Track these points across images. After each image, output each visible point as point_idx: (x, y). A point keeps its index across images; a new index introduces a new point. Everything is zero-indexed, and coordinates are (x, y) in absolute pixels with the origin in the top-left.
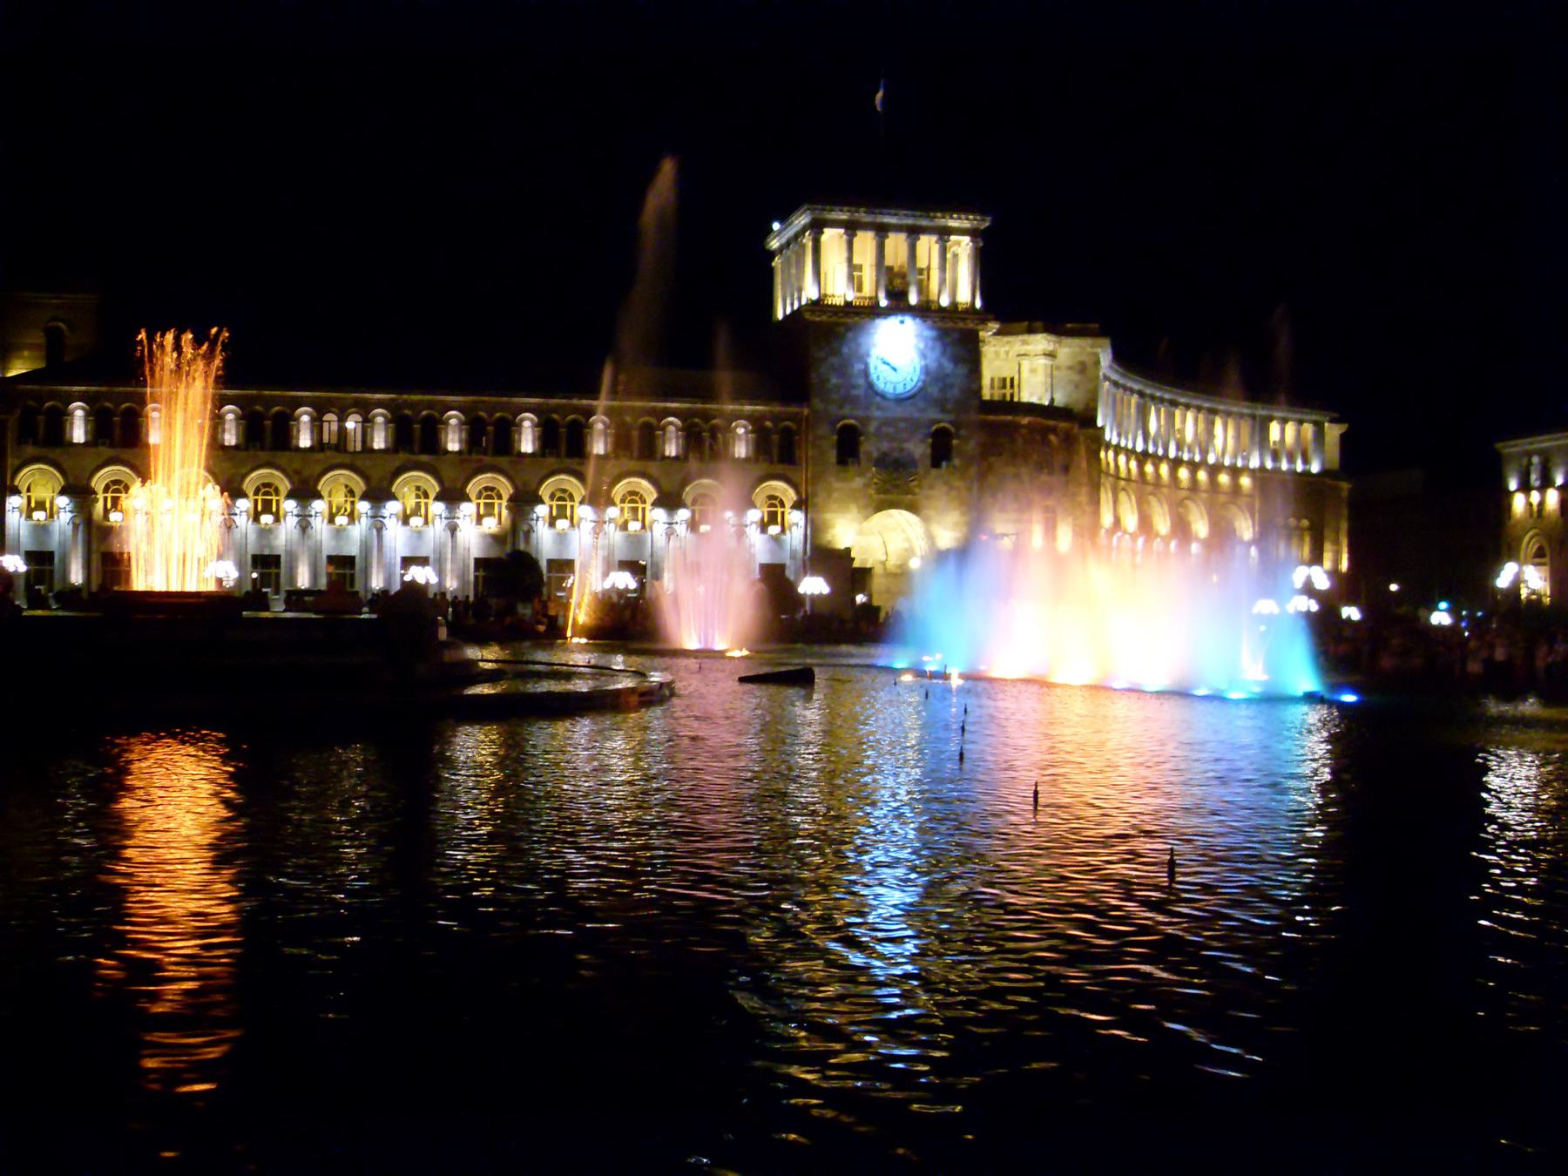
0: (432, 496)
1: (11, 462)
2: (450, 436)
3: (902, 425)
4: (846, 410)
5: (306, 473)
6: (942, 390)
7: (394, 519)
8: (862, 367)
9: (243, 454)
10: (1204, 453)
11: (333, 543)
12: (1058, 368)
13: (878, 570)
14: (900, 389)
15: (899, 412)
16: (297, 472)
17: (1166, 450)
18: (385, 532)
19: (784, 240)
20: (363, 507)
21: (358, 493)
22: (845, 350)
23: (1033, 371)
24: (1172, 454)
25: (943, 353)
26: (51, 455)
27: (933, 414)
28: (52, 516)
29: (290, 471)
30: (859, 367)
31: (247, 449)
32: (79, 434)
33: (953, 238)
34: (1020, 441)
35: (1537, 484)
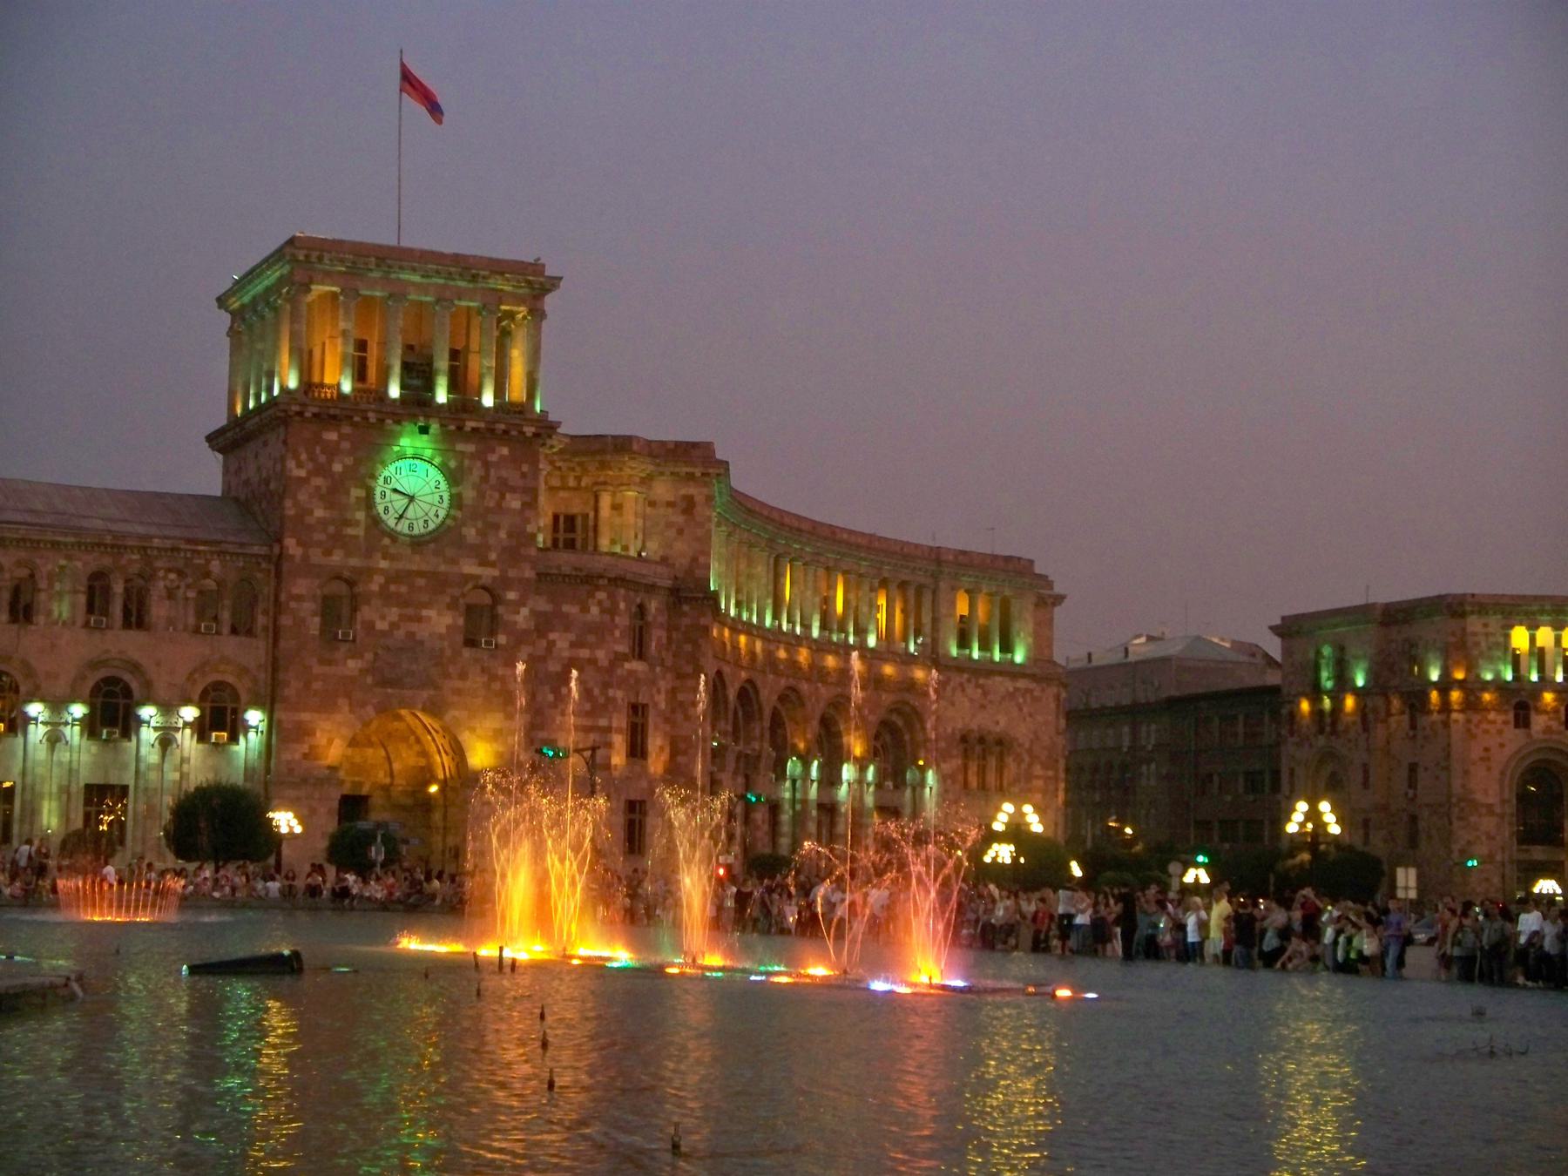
3: (421, 582)
4: (337, 557)
6: (482, 533)
8: (361, 493)
10: (861, 632)
12: (652, 504)
13: (377, 800)
14: (419, 529)
15: (416, 563)
17: (807, 627)
19: (246, 299)
22: (337, 467)
23: (617, 507)
24: (815, 633)
25: (485, 479)
27: (469, 568)
30: (357, 492)
33: (503, 307)
34: (595, 610)
35: (1329, 685)
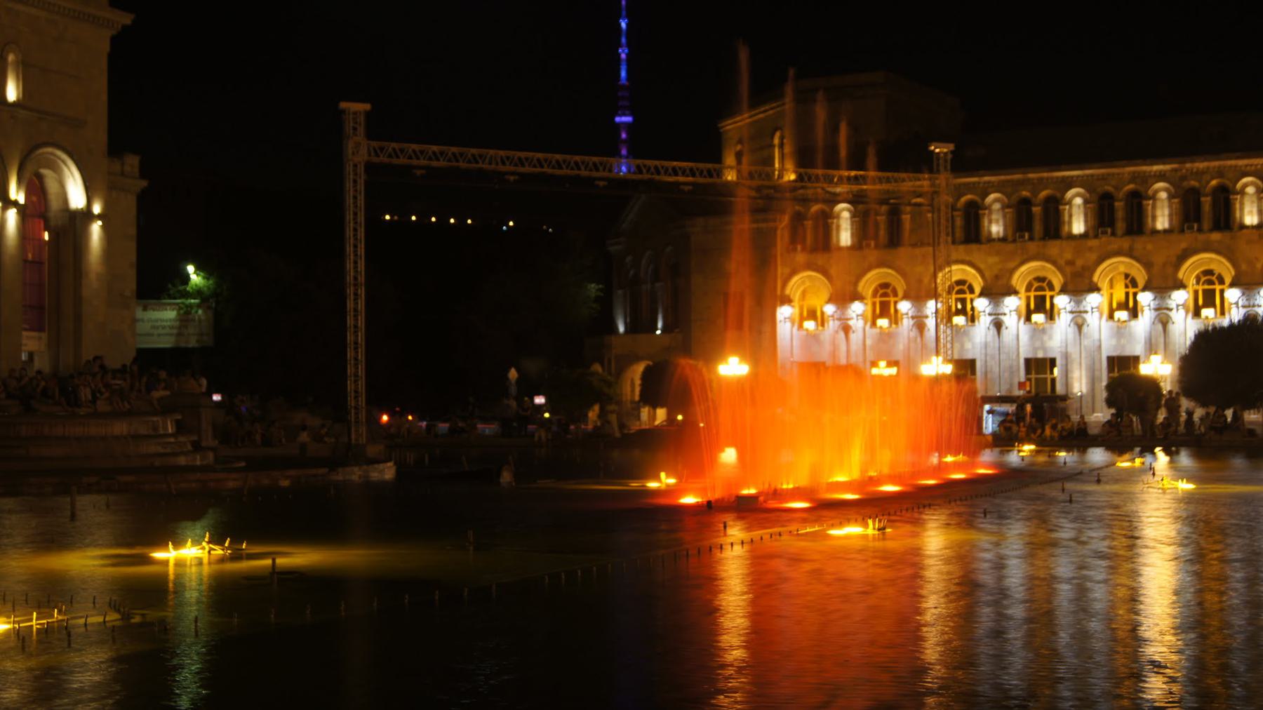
0: (1228, 280)
1: (781, 270)
2: (1247, 209)
5: (1079, 263)
7: (1182, 311)
9: (1011, 247)
11: (1114, 342)
16: (1071, 263)
18: (1170, 327)
20: (1145, 298)
21: (1141, 283)
26: (820, 262)
28: (823, 325)
29: (1062, 262)
31: (1014, 241)
32: (845, 237)
